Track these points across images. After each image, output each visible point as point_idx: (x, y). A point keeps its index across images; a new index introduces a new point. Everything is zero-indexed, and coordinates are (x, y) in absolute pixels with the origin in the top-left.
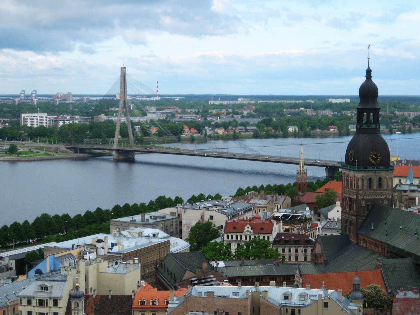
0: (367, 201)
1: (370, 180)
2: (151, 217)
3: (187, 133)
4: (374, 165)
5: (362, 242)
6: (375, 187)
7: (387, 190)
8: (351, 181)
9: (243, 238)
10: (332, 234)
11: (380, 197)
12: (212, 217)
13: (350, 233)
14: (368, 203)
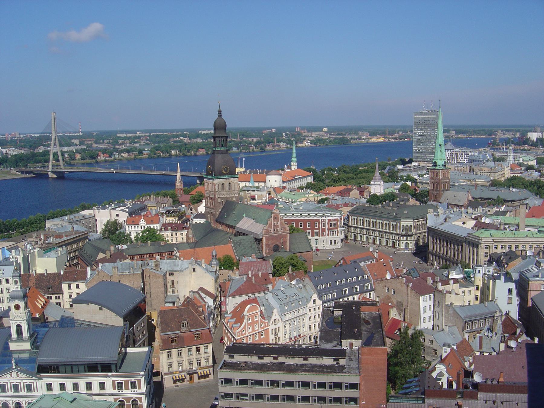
0: (222, 198)
3: (101, 158)
6: (227, 189)
9: (140, 228)
12: (117, 215)
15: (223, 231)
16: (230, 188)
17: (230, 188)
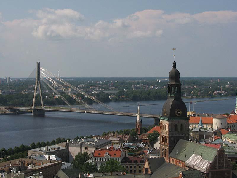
0: (174, 137)
1: (176, 125)
2: (51, 148)
4: (179, 117)
5: (171, 161)
6: (179, 129)
7: (185, 131)
8: (165, 126)
10: (155, 157)
11: (182, 135)
13: (165, 156)
14: (175, 139)
15: (174, 165)
16: (181, 129)
17: (181, 129)
